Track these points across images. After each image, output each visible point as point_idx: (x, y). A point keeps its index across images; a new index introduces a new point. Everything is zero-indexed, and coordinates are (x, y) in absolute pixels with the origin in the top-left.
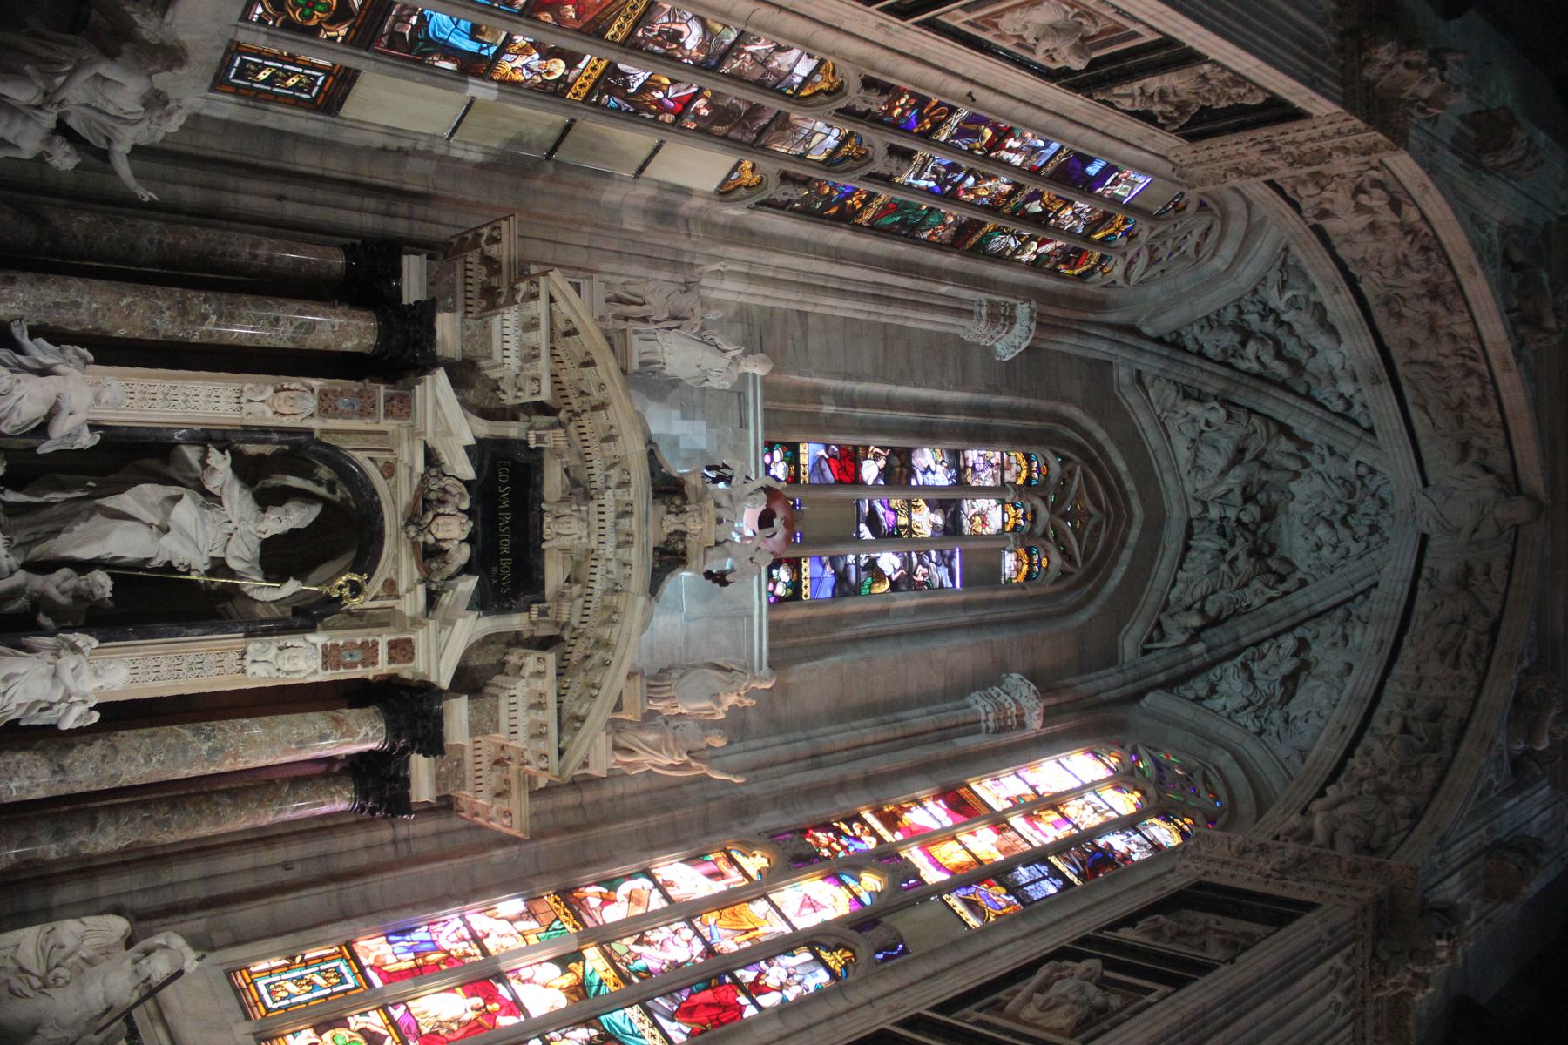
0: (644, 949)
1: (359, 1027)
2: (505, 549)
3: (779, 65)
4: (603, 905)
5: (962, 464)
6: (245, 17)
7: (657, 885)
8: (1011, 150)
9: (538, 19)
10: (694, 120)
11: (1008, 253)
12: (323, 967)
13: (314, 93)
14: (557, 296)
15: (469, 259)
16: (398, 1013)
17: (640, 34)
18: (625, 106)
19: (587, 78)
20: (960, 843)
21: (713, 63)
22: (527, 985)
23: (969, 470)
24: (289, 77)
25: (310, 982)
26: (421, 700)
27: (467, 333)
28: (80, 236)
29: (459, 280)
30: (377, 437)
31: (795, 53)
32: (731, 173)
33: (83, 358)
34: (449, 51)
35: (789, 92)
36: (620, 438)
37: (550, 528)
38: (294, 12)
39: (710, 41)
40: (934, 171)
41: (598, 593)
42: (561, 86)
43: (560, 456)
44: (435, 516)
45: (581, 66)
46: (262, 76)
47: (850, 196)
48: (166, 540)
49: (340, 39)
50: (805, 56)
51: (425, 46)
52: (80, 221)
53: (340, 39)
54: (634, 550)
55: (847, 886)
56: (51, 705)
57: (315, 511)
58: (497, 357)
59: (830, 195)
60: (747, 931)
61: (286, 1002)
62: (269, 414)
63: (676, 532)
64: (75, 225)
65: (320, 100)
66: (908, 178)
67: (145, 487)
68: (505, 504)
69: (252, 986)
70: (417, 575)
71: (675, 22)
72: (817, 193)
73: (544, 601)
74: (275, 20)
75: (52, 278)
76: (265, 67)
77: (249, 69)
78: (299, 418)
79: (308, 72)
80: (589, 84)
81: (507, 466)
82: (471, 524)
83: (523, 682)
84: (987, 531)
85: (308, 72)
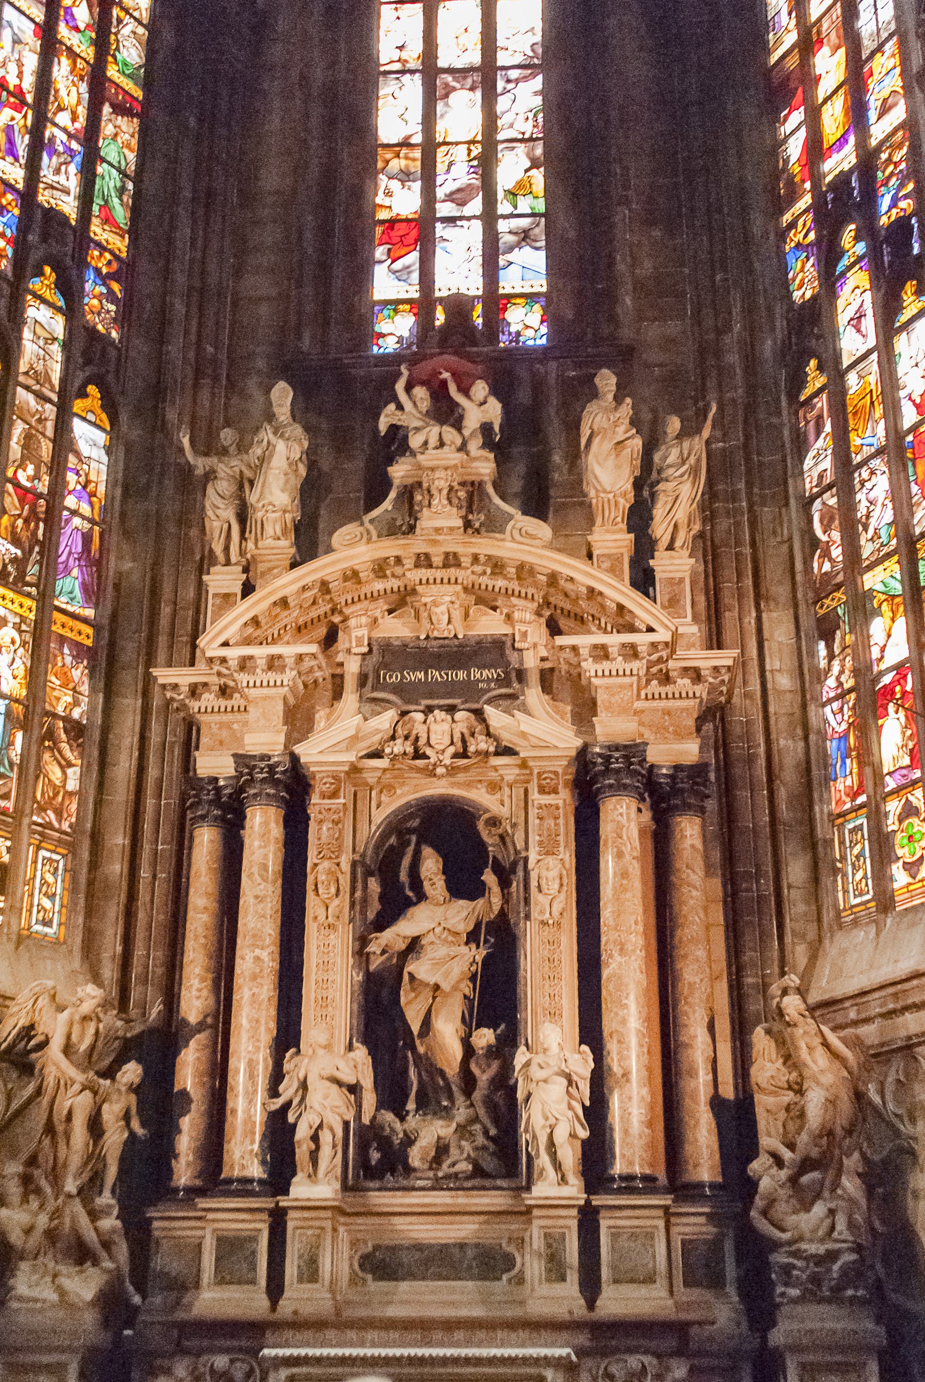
0: (873, 523)
1: (897, 823)
4: (831, 560)
5: (397, 66)
7: (820, 495)
8: (20, 75)
11: (141, 30)
12: (848, 844)
14: (221, 640)
15: (196, 710)
16: (891, 784)
18: (35, 556)
20: (825, 101)
22: (886, 654)
23: (404, 55)
24: (46, 882)
25: (858, 857)
26: (595, 764)
29: (217, 718)
30: (359, 802)
32: (89, 422)
33: (292, 1057)
36: (356, 567)
37: (443, 629)
40: (57, 171)
42: (24, 627)
43: (375, 620)
44: (430, 746)
47: (98, 271)
48: (445, 986)
49: (8, 843)
55: (850, 268)
56: (570, 1082)
57: (428, 851)
59: (99, 297)
60: (872, 403)
61: (870, 882)
62: (336, 902)
63: (449, 499)
66: (69, 206)
67: (403, 1000)
68: (421, 675)
69: (855, 910)
73: (514, 635)
75: (230, 1079)
78: (340, 877)
79: (39, 866)
80: (18, 599)
82: (437, 712)
83: (583, 664)
84: (477, 27)
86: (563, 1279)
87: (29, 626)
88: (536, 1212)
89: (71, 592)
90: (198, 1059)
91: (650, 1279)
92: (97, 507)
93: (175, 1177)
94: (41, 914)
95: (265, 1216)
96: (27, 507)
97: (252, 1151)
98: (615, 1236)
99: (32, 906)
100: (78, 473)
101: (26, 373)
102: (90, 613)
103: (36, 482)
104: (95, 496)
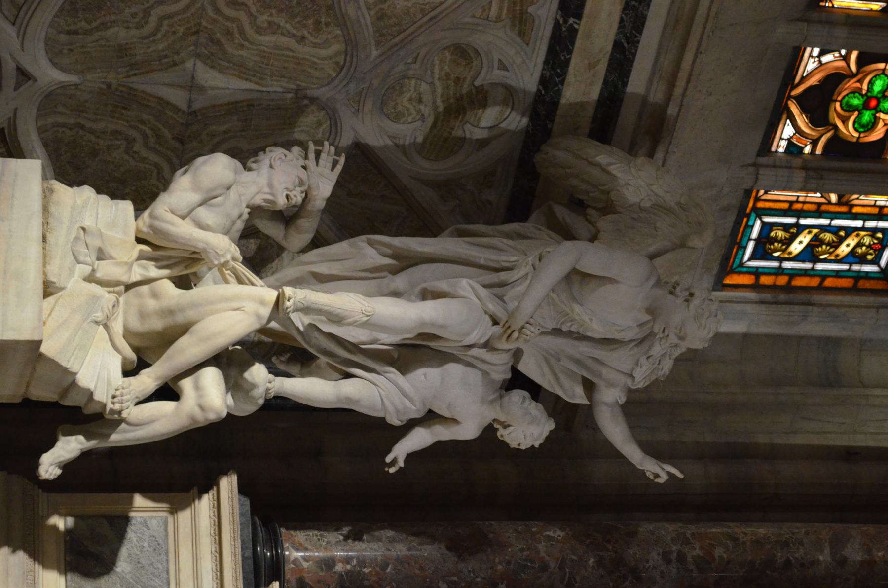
24: (841, 240)
28: (552, 564)
38: (845, 121)
46: (796, 247)
52: (549, 538)
64: (541, 547)
74: (815, 143)
76: (801, 229)
77: (775, 239)
79: (871, 224)
85: (871, 224)
90: (544, 568)
93: (300, 536)
94: (781, 234)
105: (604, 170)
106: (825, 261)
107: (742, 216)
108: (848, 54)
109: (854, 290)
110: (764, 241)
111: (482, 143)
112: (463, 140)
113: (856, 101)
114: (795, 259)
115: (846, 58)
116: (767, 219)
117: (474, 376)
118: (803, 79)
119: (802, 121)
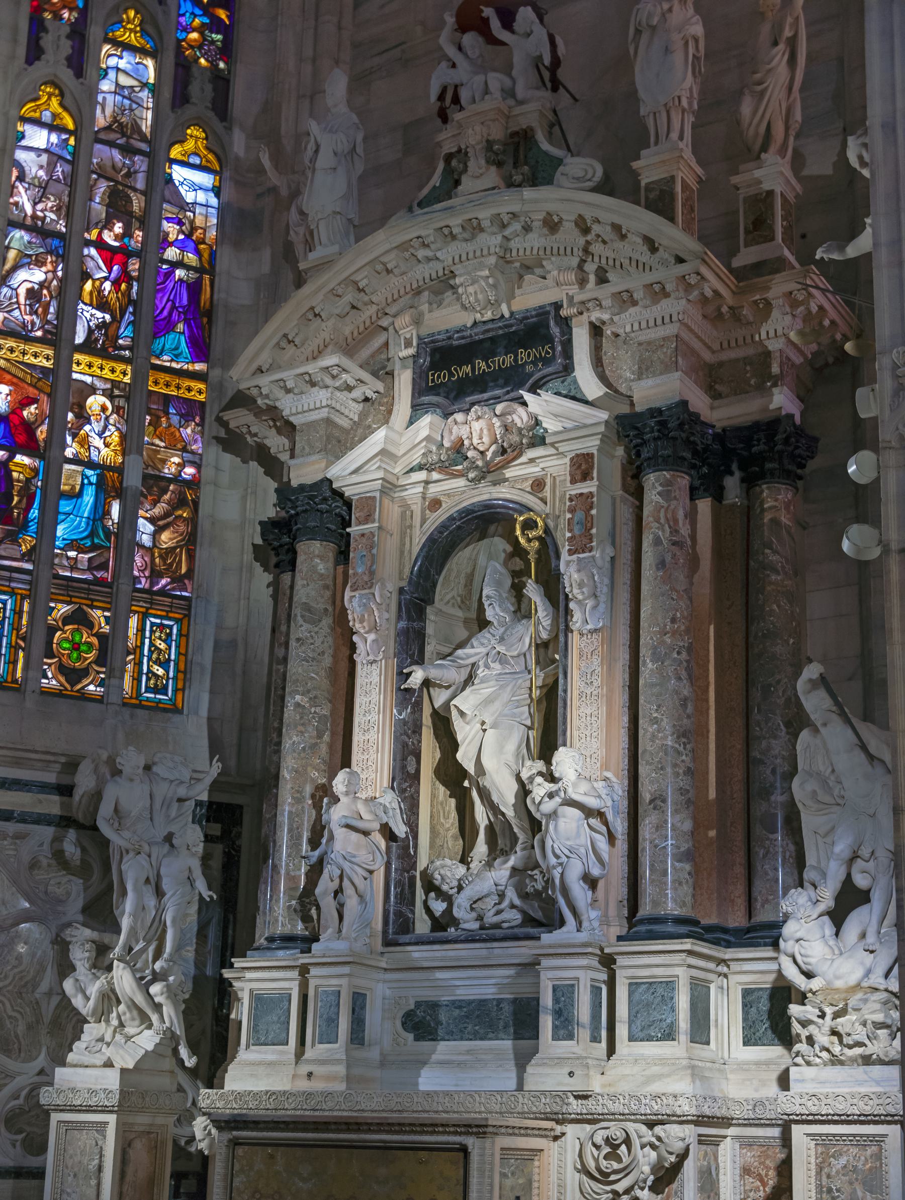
2: (509, 359)
3: (41, 167)
6: (100, 700)
9: (45, 441)
10: (131, 236)
13: (171, 623)
17: (39, 333)
18: (128, 317)
19: (102, 369)
21: (56, 242)
24: (157, 648)
27: (307, 449)
31: (20, 155)
34: (100, 512)
35: (72, 141)
38: (86, 659)
39: (30, 256)
41: (542, 242)
42: (117, 392)
45: (88, 380)
46: (161, 672)
49: (107, 614)
50: (24, 143)
51: (98, 536)
53: (107, 614)
54: (480, 216)
58: (324, 413)
65: (177, 616)
68: (468, 369)
70: (523, 459)
71: (18, 302)
72: (200, 47)
74: (98, 673)
77: (156, 685)
79: (147, 634)
80: (108, 365)
81: (433, 375)
85: (147, 634)
86: (570, 1037)
87: (124, 390)
88: (545, 962)
89: (176, 349)
91: (669, 1035)
92: (206, 255)
94: (152, 682)
95: (295, 974)
96: (116, 268)
97: (290, 907)
98: (633, 987)
99: (140, 673)
100: (180, 223)
101: (108, 128)
102: (199, 367)
103: (126, 240)
104: (204, 242)
105: (83, 796)
106: (169, 655)
107: (135, 704)
108: (46, 664)
109: (187, 636)
110: (156, 690)
111: (84, 850)
112: (82, 860)
113: (75, 655)
114: (168, 672)
115: (50, 665)
116: (143, 690)
117: (165, 862)
118: (62, 685)
119: (85, 682)
